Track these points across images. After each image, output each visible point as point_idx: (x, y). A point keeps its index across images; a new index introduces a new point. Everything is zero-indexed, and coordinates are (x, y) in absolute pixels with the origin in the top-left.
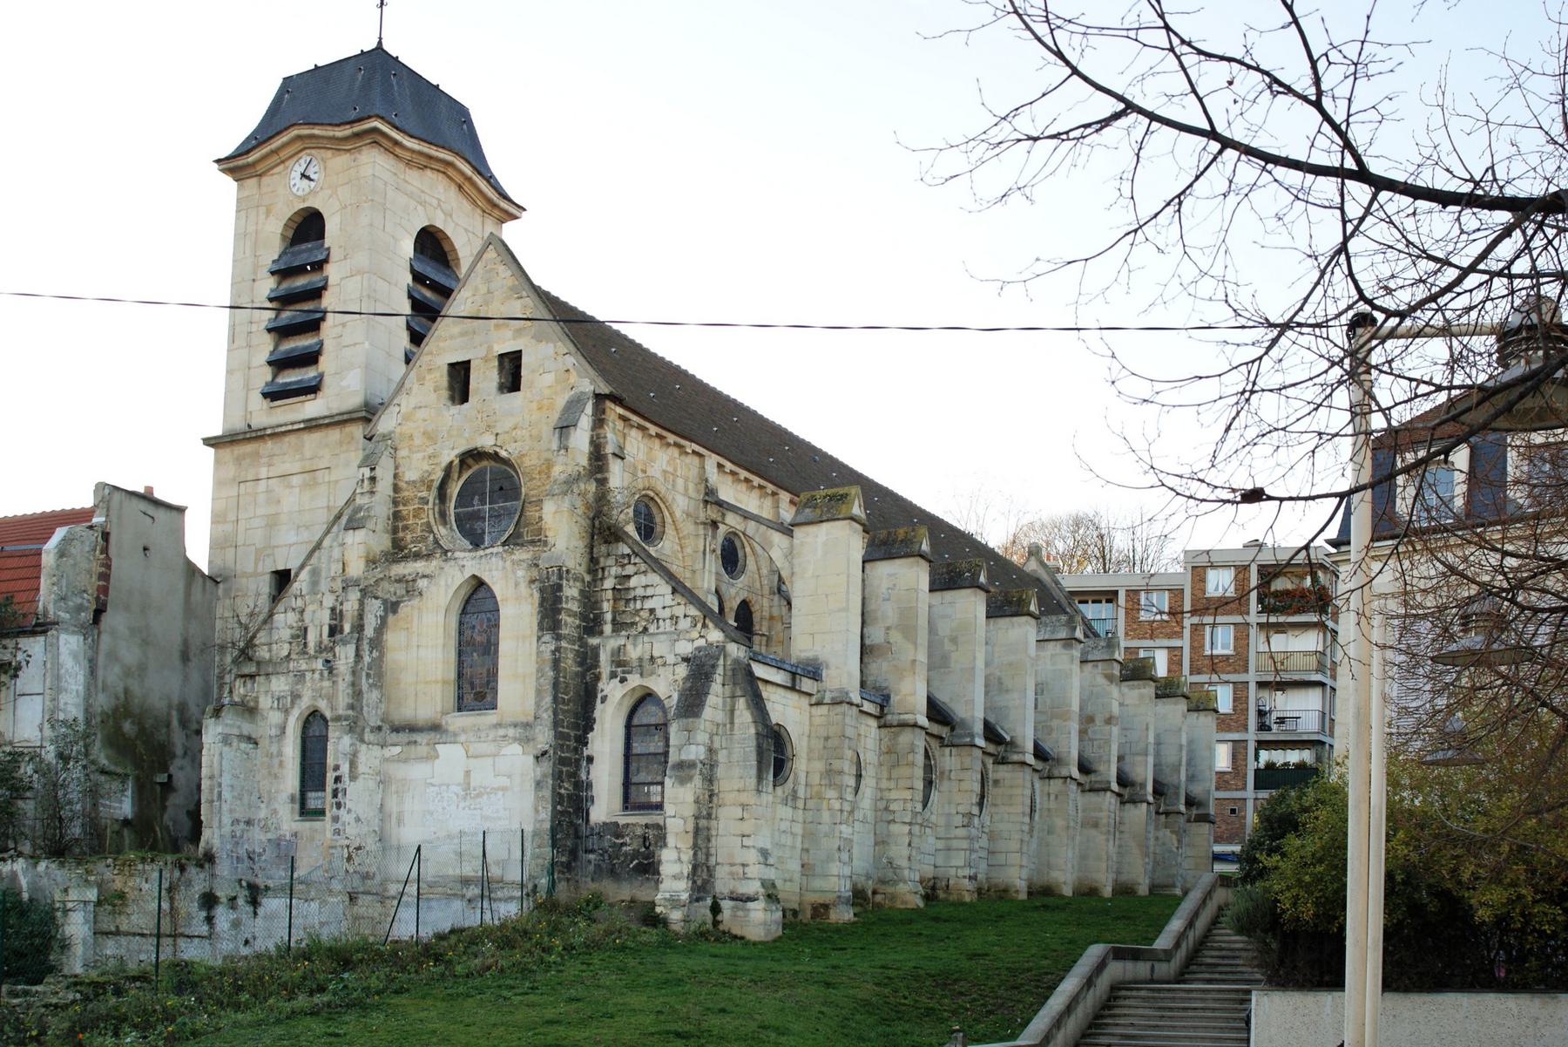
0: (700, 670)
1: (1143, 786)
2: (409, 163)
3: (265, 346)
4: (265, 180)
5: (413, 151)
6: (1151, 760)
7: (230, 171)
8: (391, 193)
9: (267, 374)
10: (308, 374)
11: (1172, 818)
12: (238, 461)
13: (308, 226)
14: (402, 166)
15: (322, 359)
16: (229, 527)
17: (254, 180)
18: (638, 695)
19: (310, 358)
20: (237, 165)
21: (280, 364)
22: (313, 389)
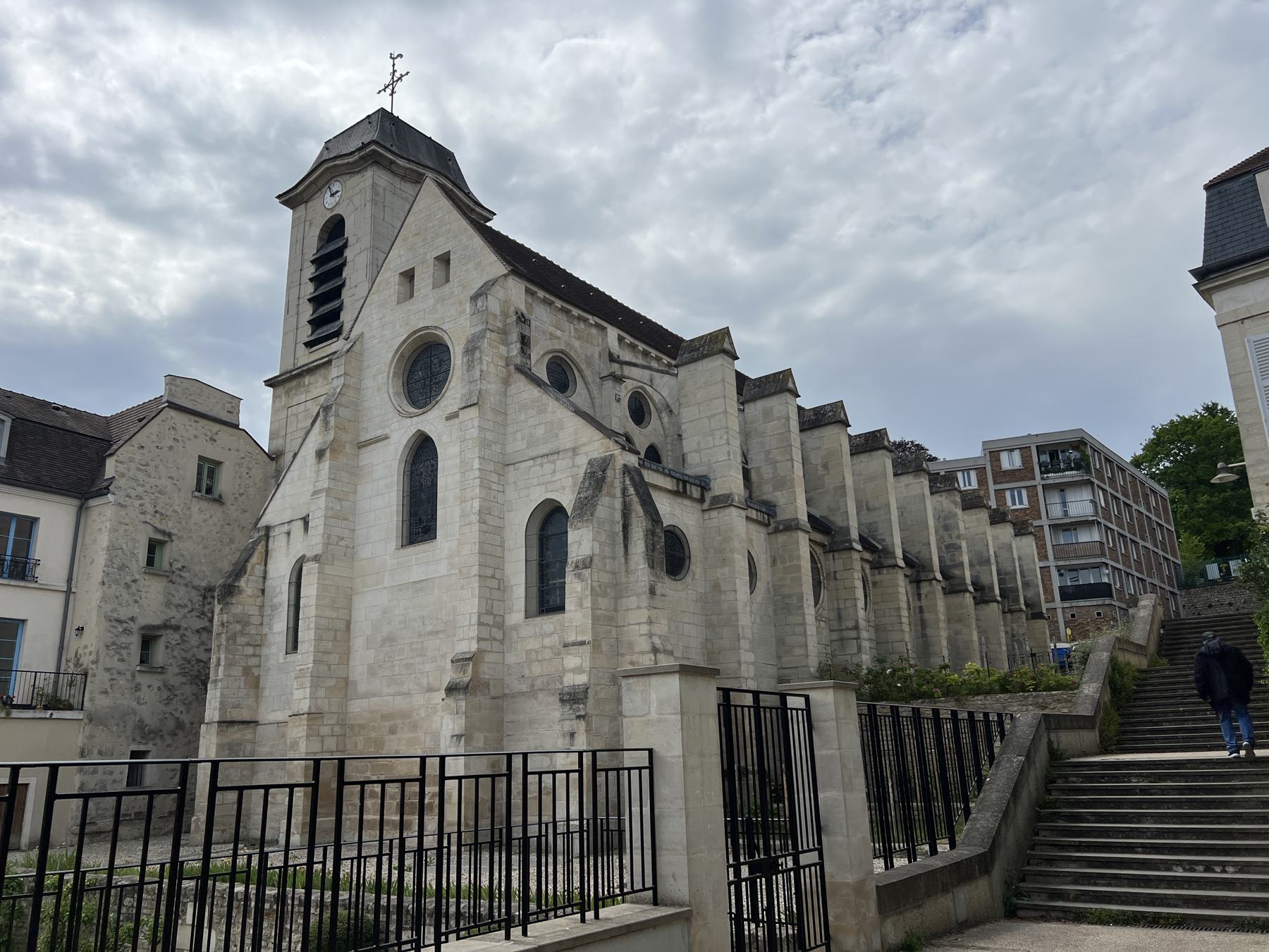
0: (596, 477)
1: (992, 589)
2: (403, 178)
3: (307, 312)
4: (310, 204)
5: (407, 169)
6: (994, 568)
7: (285, 203)
8: (388, 195)
9: (308, 330)
10: (332, 328)
11: (1016, 615)
12: (287, 393)
13: (335, 228)
14: (397, 181)
15: (342, 314)
16: (280, 442)
17: (303, 206)
18: (548, 509)
19: (335, 315)
20: (291, 199)
21: (316, 323)
22: (337, 334)
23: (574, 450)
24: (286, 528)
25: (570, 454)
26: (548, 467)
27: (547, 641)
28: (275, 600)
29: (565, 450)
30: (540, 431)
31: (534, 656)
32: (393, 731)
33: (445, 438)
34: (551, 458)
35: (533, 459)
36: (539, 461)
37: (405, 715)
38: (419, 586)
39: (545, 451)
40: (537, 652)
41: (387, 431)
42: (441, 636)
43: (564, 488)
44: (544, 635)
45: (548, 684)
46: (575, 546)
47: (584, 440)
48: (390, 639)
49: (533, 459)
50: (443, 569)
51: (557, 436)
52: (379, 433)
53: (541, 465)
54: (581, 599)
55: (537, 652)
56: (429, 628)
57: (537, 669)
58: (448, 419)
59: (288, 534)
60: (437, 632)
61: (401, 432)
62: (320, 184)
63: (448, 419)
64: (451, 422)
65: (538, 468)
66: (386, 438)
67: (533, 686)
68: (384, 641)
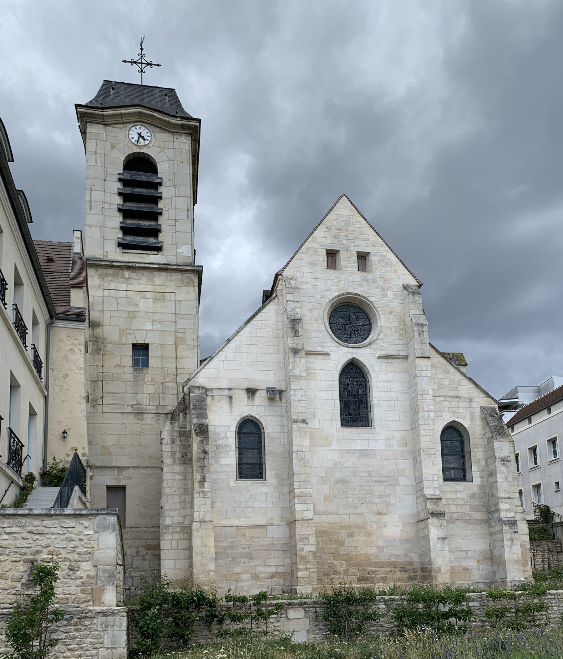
23: (471, 400)
24: (226, 392)
25: (468, 400)
26: (454, 404)
27: (459, 495)
28: (220, 442)
29: (465, 398)
30: (446, 382)
31: (451, 502)
32: (351, 535)
33: (376, 369)
34: (456, 399)
35: (444, 397)
36: (448, 399)
37: (359, 527)
38: (364, 453)
39: (450, 395)
40: (453, 500)
41: (326, 350)
42: (385, 484)
43: (465, 417)
44: (457, 492)
45: (461, 517)
46: (499, 450)
47: (474, 395)
48: (343, 481)
49: (444, 397)
50: (380, 446)
51: (457, 388)
52: (319, 349)
53: (450, 402)
54: (507, 477)
55: (453, 500)
56: (375, 478)
57: (453, 509)
58: (379, 357)
59: (231, 397)
60: (382, 482)
61: (341, 354)
62: (125, 119)
63: (379, 357)
64: (382, 360)
65: (448, 403)
66: (328, 354)
67: (451, 517)
68: (338, 482)
